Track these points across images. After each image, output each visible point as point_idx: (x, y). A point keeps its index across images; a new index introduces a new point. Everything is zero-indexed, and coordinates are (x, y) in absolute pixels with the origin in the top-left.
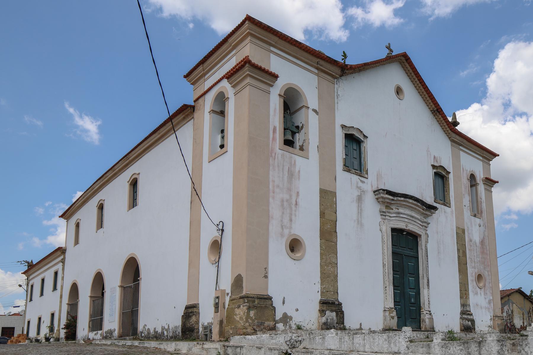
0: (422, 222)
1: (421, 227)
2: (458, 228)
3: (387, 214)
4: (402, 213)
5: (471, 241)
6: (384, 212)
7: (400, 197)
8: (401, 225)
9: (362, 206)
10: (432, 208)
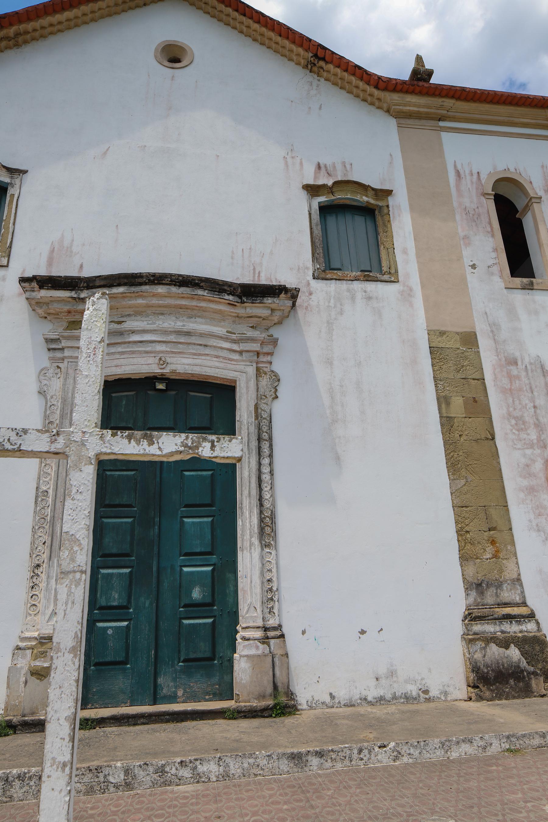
0: (234, 341)
1: (236, 357)
6: (53, 341)
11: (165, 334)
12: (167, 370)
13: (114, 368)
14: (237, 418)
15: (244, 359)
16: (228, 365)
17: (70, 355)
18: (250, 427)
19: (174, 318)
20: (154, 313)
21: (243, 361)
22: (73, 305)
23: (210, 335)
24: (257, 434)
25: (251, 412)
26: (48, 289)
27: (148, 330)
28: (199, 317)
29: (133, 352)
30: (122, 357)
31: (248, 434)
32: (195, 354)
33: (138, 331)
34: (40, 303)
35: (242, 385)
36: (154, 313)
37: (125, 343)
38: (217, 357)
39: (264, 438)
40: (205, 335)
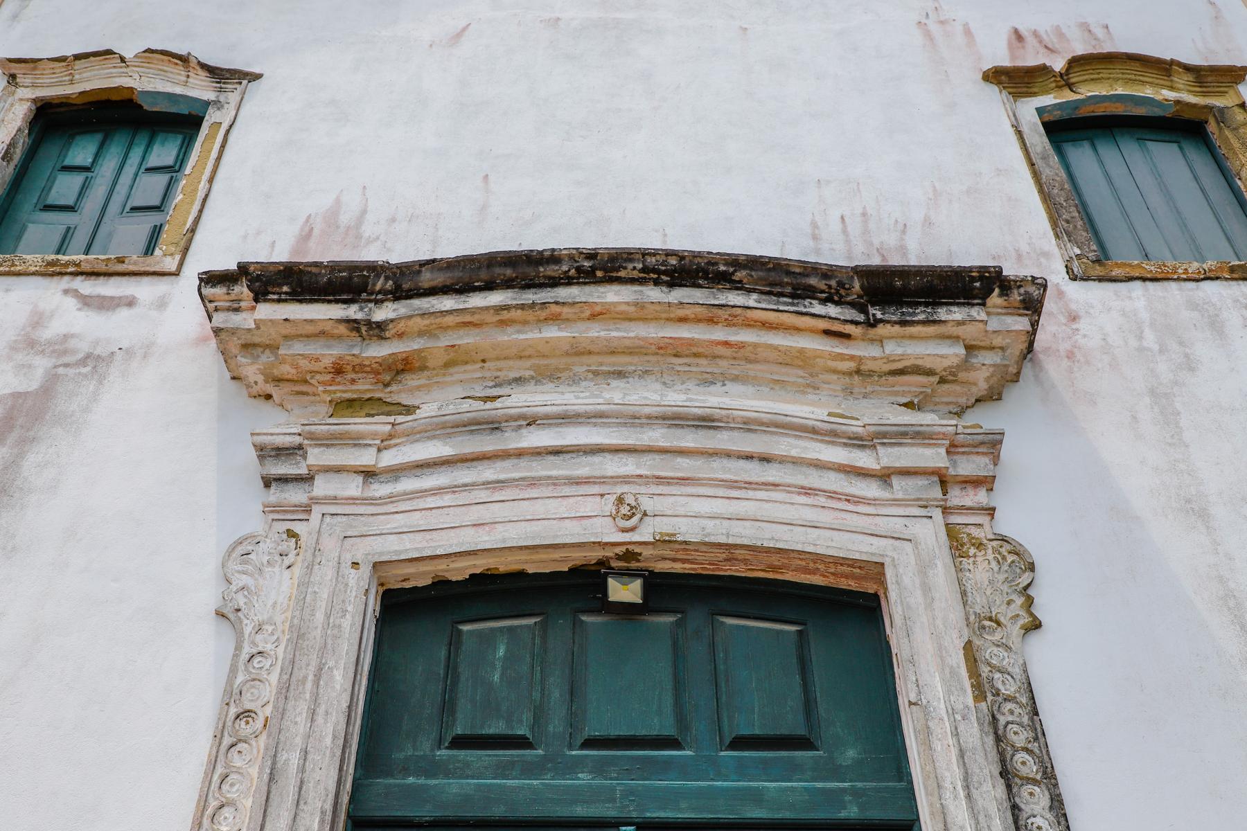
1: (871, 489)
3: (317, 456)
6: (281, 452)
9: (32, 459)
11: (633, 425)
12: (645, 534)
13: (471, 531)
14: (906, 692)
15: (900, 495)
16: (844, 515)
17: (331, 493)
18: (961, 728)
19: (658, 386)
21: (896, 502)
22: (353, 346)
23: (777, 425)
24: (993, 755)
26: (279, 301)
27: (578, 415)
28: (735, 379)
29: (533, 482)
30: (497, 496)
31: (962, 754)
32: (733, 484)
34: (255, 345)
35: (907, 581)
36: (596, 373)
37: (505, 455)
38: (807, 491)
39: (1024, 771)
40: (762, 424)
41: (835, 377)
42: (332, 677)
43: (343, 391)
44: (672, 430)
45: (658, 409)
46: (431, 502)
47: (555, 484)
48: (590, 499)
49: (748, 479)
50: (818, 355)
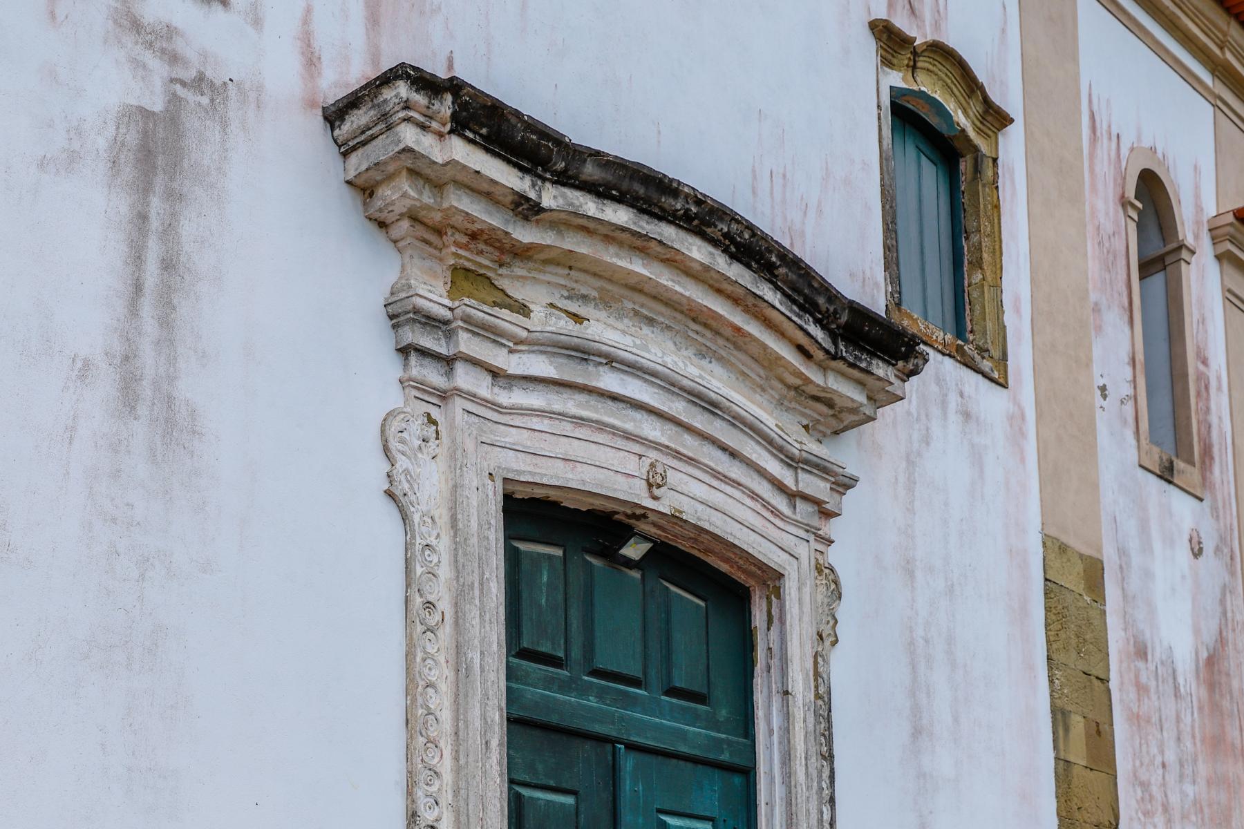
0: (793, 462)
1: (781, 503)
2: (1055, 548)
3: (467, 343)
4: (611, 361)
5: (1141, 652)
7: (599, 191)
8: (595, 466)
10: (874, 342)
13: (560, 464)
15: (798, 517)
20: (636, 313)
21: (796, 524)
23: (752, 428)
25: (807, 675)
28: (720, 359)
29: (601, 426)
32: (716, 475)
33: (622, 362)
36: (636, 313)
38: (754, 496)
41: (780, 386)
42: (489, 588)
43: (468, 258)
44: (690, 405)
45: (690, 383)
46: (535, 423)
47: (614, 434)
48: (632, 456)
49: (727, 474)
50: (787, 365)
